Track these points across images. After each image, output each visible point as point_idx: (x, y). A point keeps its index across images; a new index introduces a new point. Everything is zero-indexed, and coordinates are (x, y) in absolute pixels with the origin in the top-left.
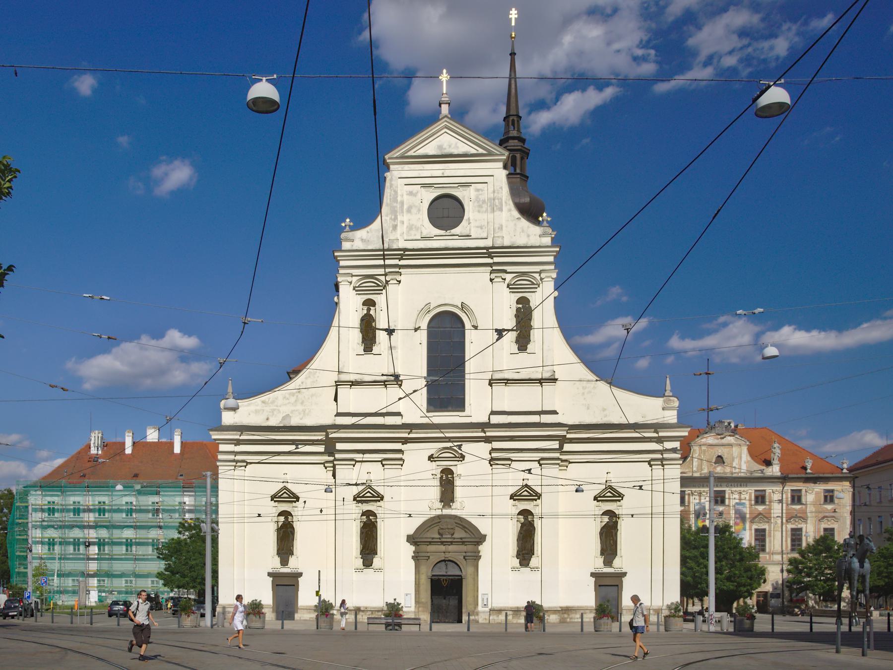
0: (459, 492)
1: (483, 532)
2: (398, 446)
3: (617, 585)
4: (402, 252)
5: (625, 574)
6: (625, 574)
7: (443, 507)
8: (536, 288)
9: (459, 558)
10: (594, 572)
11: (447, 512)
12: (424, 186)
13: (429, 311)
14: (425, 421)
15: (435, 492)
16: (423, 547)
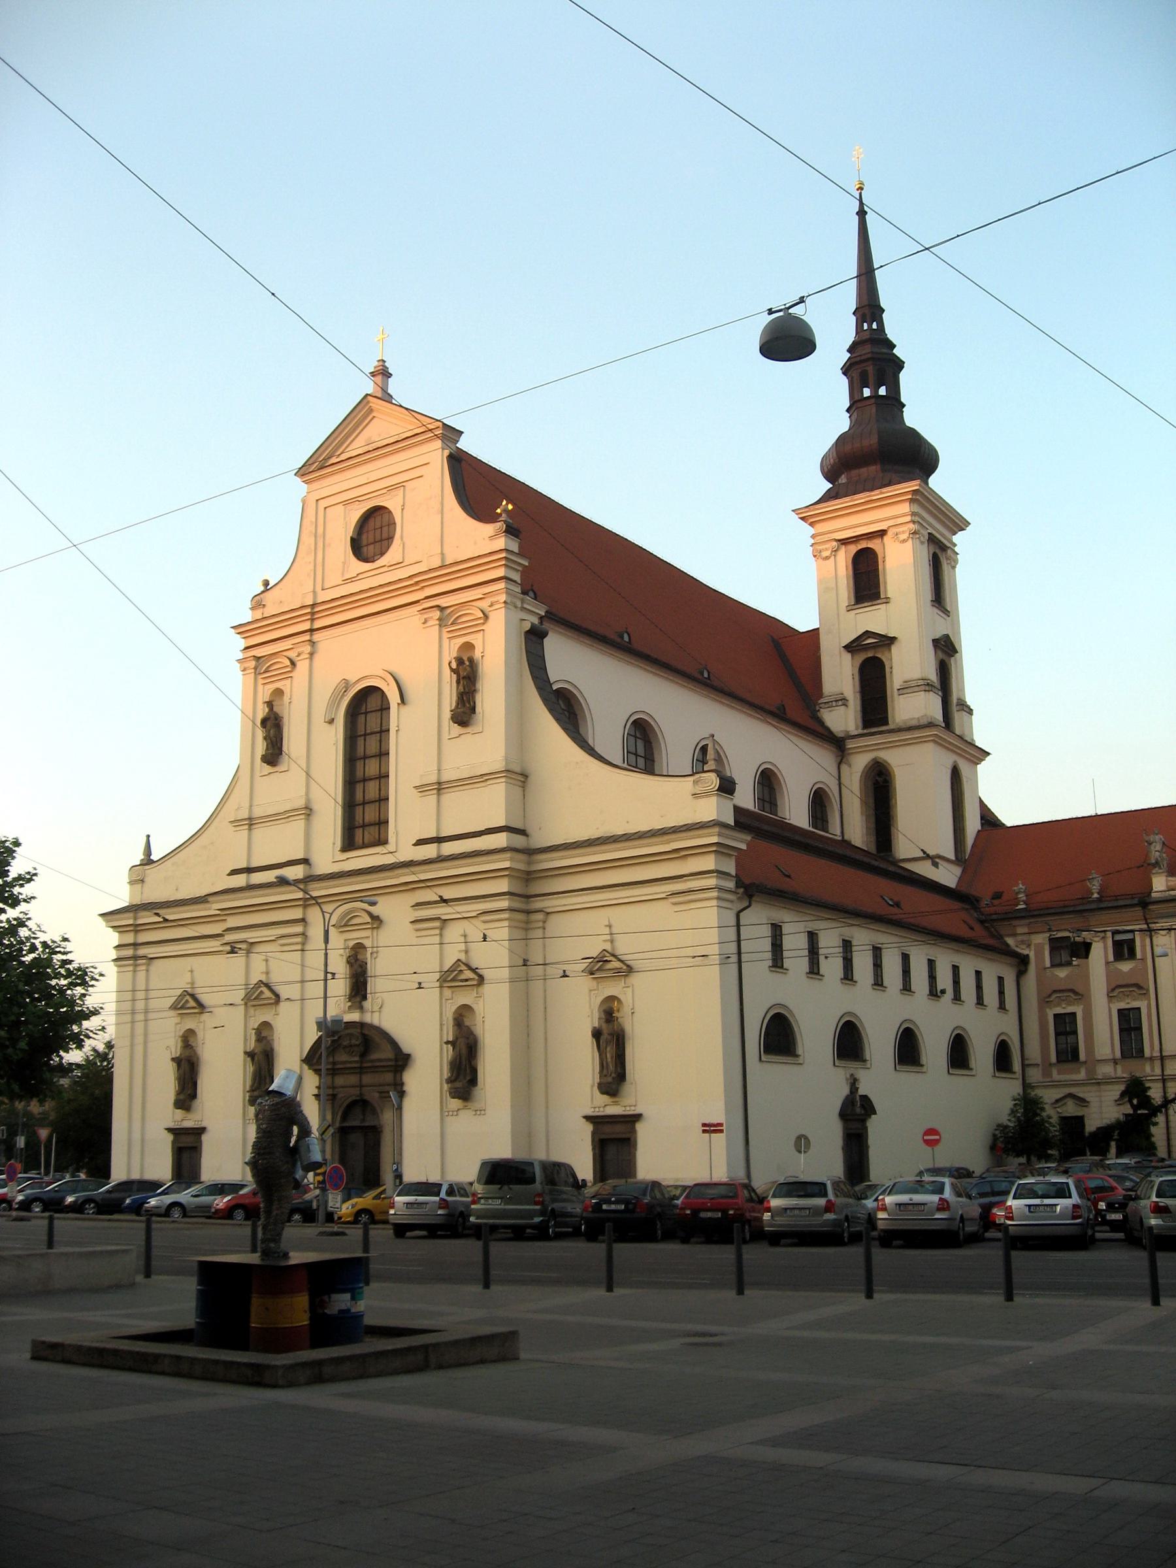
0: (375, 986)
1: (406, 1049)
2: (297, 914)
3: (629, 1139)
4: (309, 610)
5: (638, 1117)
6: (638, 1117)
7: (350, 1007)
8: (484, 624)
9: (372, 1096)
10: (590, 1112)
11: (354, 1017)
12: (346, 503)
13: (345, 691)
14: (336, 868)
15: (340, 987)
16: (340, 1081)
